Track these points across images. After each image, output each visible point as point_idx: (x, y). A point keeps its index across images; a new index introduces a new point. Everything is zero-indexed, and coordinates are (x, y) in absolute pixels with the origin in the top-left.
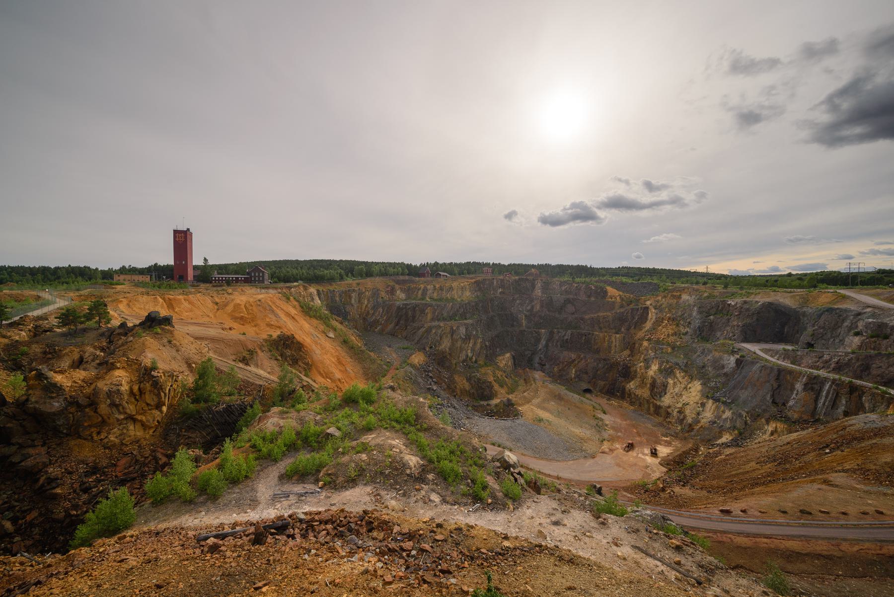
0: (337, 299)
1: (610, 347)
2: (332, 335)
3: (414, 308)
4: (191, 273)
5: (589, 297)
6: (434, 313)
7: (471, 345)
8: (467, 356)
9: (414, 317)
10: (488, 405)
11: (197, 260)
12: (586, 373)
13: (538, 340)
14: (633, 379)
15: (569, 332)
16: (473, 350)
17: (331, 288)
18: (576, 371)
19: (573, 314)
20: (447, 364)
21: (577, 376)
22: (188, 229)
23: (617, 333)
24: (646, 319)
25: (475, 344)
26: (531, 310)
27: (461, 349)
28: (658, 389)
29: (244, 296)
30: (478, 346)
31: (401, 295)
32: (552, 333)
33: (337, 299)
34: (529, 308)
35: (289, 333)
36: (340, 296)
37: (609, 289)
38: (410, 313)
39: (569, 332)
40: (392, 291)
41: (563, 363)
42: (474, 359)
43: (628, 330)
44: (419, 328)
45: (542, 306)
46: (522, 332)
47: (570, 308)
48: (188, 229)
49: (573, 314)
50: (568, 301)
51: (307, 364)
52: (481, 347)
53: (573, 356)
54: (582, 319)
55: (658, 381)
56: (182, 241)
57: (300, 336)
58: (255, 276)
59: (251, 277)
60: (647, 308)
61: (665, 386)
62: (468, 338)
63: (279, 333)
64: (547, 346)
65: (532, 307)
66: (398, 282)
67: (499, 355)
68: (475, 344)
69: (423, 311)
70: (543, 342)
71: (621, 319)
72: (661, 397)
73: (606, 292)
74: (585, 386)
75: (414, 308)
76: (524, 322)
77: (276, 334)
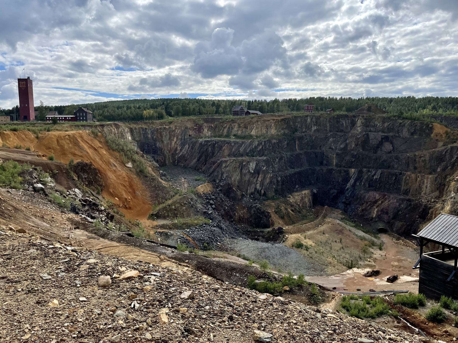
0: (149, 136)
1: (420, 188)
2: (130, 165)
3: (214, 145)
4: (32, 115)
5: (412, 134)
6: (231, 150)
7: (260, 179)
8: (256, 189)
9: (213, 153)
10: (261, 232)
11: (37, 104)
12: (387, 213)
13: (347, 180)
15: (379, 171)
16: (262, 184)
17: (144, 126)
18: (377, 212)
19: (390, 152)
20: (232, 195)
21: (378, 216)
22: (29, 78)
23: (430, 173)
25: (264, 178)
26: (345, 148)
27: (249, 183)
29: (66, 131)
30: (268, 180)
31: (206, 132)
32: (360, 172)
33: (149, 136)
34: (342, 146)
35: (88, 162)
36: (152, 133)
38: (210, 149)
39: (379, 171)
40: (199, 129)
41: (367, 203)
42: (263, 192)
43: (444, 170)
44: (214, 163)
45: (356, 145)
46: (330, 171)
47: (388, 147)
48: (29, 78)
50: (386, 139)
51: (101, 186)
52: (271, 182)
53: (377, 196)
54: (397, 158)
56: (25, 87)
57: (98, 163)
58: (80, 116)
59: (76, 117)
62: (257, 172)
63: (79, 160)
64: (354, 185)
65: (347, 145)
66: (206, 121)
67: (296, 192)
68: (264, 178)
69: (220, 148)
70: (352, 181)
73: (431, 129)
74: (381, 226)
75: (214, 145)
77: (76, 161)
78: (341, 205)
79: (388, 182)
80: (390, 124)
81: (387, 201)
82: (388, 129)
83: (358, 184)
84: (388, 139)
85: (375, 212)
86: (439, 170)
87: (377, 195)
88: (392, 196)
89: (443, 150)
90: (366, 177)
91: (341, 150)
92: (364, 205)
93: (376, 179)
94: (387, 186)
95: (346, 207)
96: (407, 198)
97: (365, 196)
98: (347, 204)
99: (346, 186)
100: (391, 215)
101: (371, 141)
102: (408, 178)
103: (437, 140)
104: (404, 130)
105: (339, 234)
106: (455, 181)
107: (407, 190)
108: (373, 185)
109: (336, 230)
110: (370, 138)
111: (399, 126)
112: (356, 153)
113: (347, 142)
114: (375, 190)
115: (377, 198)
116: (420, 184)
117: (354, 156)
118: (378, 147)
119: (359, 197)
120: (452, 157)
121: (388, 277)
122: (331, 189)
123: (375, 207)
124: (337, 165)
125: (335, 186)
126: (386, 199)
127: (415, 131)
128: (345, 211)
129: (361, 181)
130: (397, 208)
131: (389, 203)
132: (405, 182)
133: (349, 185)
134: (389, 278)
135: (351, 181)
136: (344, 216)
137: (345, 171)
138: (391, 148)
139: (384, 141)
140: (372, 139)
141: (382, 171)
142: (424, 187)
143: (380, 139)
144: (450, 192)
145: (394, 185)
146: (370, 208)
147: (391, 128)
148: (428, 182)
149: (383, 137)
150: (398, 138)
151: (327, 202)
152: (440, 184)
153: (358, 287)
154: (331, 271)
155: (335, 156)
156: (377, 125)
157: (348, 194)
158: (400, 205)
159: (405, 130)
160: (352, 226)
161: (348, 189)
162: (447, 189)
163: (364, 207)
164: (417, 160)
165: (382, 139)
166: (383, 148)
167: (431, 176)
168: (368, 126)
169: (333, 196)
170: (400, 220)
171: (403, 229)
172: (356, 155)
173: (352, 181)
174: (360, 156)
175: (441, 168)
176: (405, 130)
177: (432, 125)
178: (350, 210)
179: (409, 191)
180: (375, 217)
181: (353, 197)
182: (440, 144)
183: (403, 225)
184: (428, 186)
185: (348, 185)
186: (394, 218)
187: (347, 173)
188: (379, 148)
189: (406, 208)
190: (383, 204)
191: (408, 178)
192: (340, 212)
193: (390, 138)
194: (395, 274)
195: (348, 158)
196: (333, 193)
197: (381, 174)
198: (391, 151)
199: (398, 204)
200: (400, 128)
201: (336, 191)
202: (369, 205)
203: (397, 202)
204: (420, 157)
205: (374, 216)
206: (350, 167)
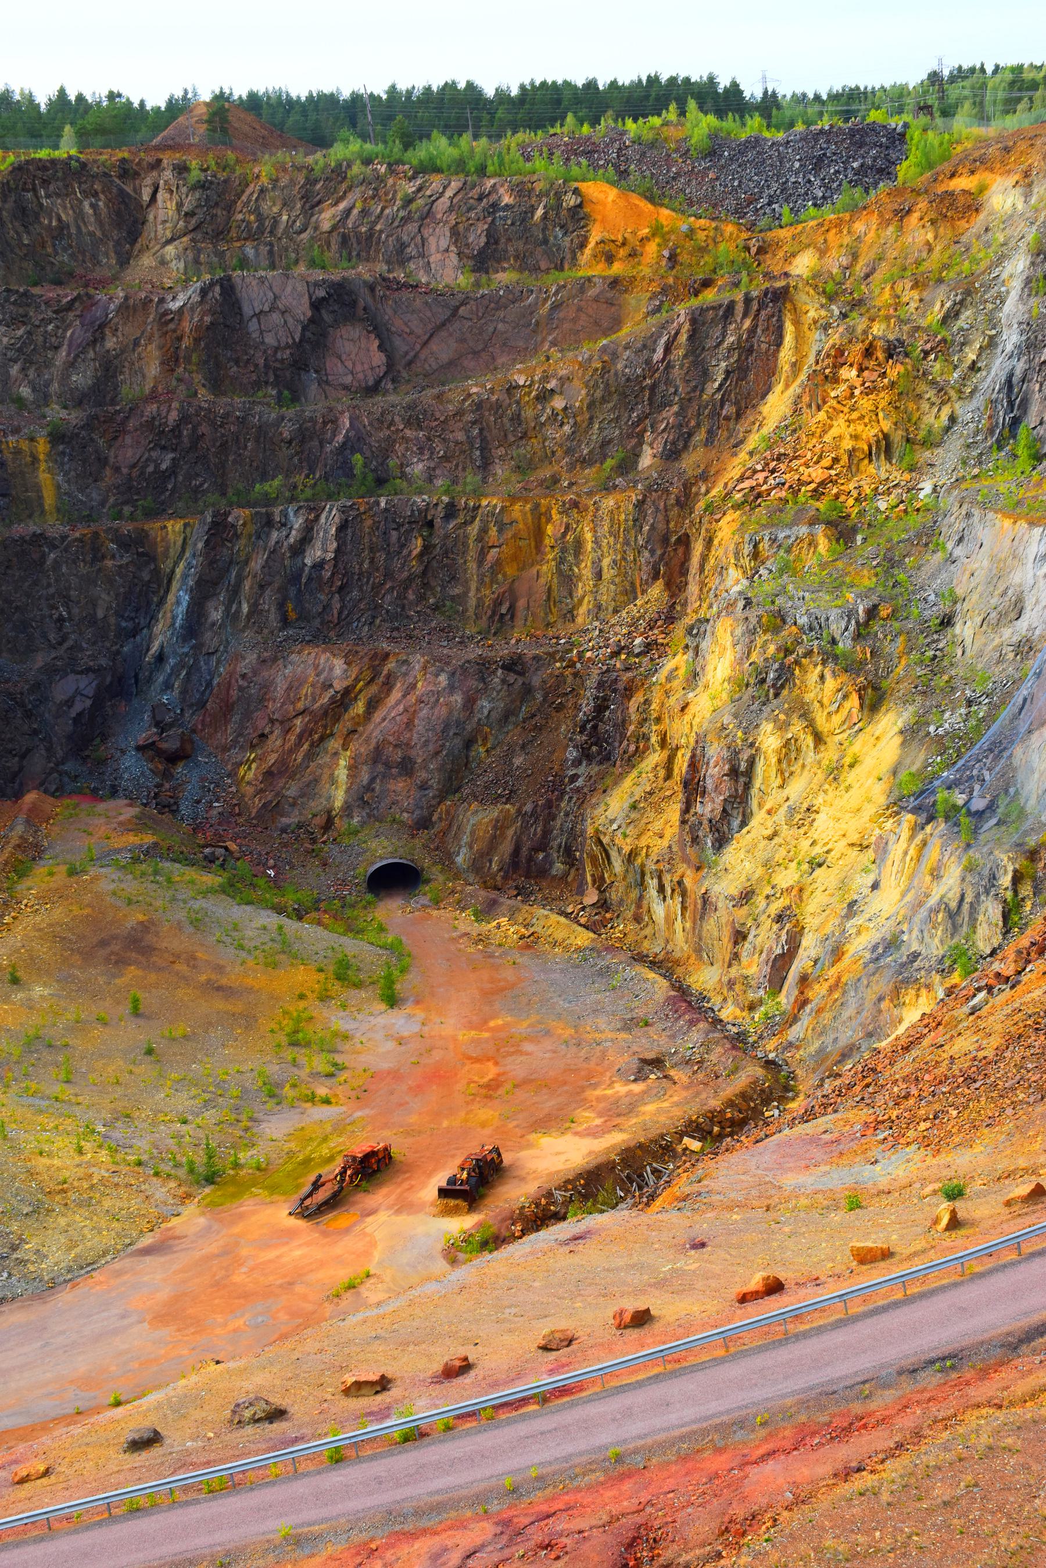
1: (568, 580)
12: (406, 767)
13: (143, 597)
14: (631, 761)
15: (330, 519)
18: (353, 768)
21: (363, 799)
23: (608, 488)
24: (770, 371)
28: (720, 801)
37: (602, 193)
41: (286, 724)
43: (672, 454)
45: (171, 360)
47: (356, 353)
49: (373, 390)
50: (336, 304)
55: (715, 751)
60: (780, 297)
61: (741, 773)
65: (110, 369)
70: (178, 601)
71: (633, 395)
72: (721, 842)
73: (578, 217)
74: (382, 850)
76: (47, 480)
78: (132, 766)
79: (388, 575)
80: (348, 212)
81: (396, 694)
82: (345, 240)
83: (216, 615)
84: (354, 304)
85: (342, 773)
86: (646, 460)
87: (339, 665)
88: (418, 660)
89: (654, 338)
90: (257, 564)
91: (79, 403)
92: (275, 741)
93: (319, 566)
94: (388, 601)
95: (167, 775)
96: (503, 651)
97: (267, 687)
98: (173, 758)
99: (150, 639)
100: (431, 773)
101: (253, 325)
102: (493, 531)
103: (615, 283)
104: (432, 241)
105: (121, 962)
106: (736, 507)
107: (498, 603)
108: (311, 608)
109: (103, 943)
110: (247, 311)
111: (405, 220)
112: (174, 416)
113: (110, 343)
114: (319, 638)
115: (339, 685)
116: (561, 561)
117: (162, 436)
118: (300, 365)
119: (234, 693)
120: (706, 375)
121: (441, 1179)
122: (52, 671)
123: (334, 744)
124: (69, 512)
125: (76, 647)
126: (388, 685)
127: (492, 236)
128: (164, 804)
129: (235, 592)
130: (458, 723)
131: (412, 699)
132: (480, 562)
133: (161, 635)
134: (452, 1181)
135: (171, 598)
136: (149, 839)
137: (125, 543)
138: (379, 359)
139: (327, 317)
140: (257, 315)
141: (343, 510)
142: (586, 571)
143: (303, 310)
144: (722, 570)
145: (426, 585)
146: (310, 756)
147: (358, 235)
148: (600, 533)
149: (321, 293)
150: (405, 295)
151: (38, 762)
152: (665, 540)
153: (133, 1419)
154: (72, 1245)
155: (42, 447)
156: (276, 221)
157: (168, 686)
158: (470, 702)
159: (438, 240)
160: (207, 892)
161: (160, 658)
162: (704, 558)
163: (272, 758)
164: (528, 413)
165: (316, 305)
166: (333, 366)
167: (609, 502)
168: (220, 234)
169: (76, 720)
170: (487, 797)
171: (506, 848)
172: (177, 429)
173: (178, 601)
174: (204, 429)
175: (659, 447)
176: (438, 240)
177: (576, 192)
178: (191, 789)
179: (512, 608)
180: (348, 809)
181: (202, 704)
182: (637, 304)
183: (499, 826)
184: (606, 562)
185: (159, 627)
186: (452, 784)
187: (141, 549)
188: (305, 368)
189: (507, 716)
190: (377, 716)
191: (493, 531)
192: (129, 812)
193: (364, 298)
194: (475, 1146)
195: (129, 452)
196: (70, 703)
197: (342, 528)
198: (378, 382)
199: (458, 698)
200: (412, 227)
201: (87, 684)
202: (300, 737)
203: (451, 688)
204: (545, 396)
205: (339, 798)
206: (156, 512)
